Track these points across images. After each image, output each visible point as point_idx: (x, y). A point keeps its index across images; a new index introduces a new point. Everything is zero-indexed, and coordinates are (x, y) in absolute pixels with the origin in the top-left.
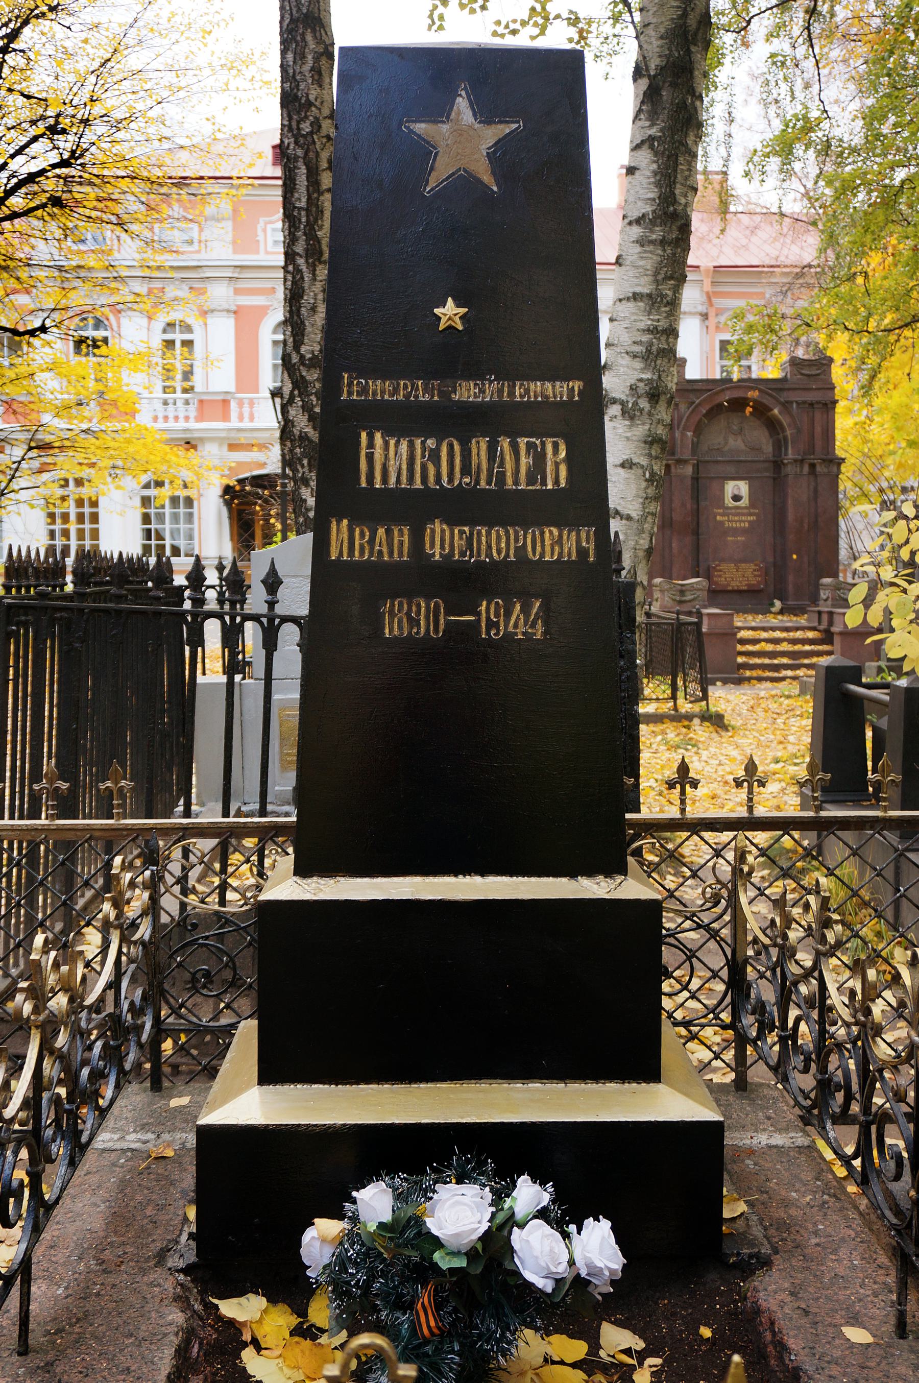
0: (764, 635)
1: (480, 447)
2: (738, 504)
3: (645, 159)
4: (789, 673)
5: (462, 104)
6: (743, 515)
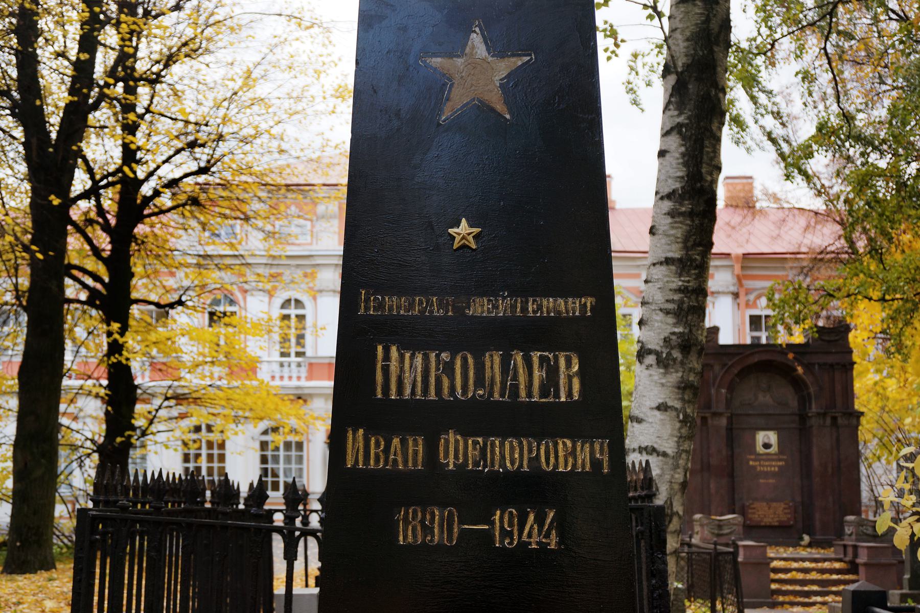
0: (795, 565)
1: (493, 361)
3: (674, 142)
4: (819, 599)
5: (476, 39)
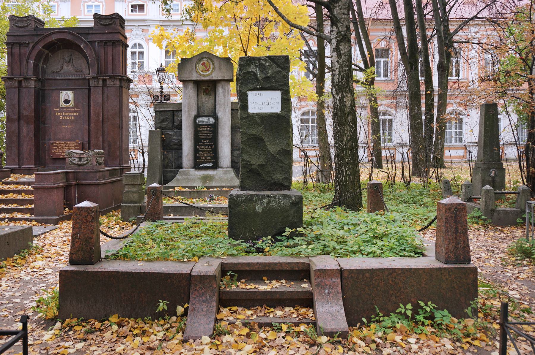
6: (71, 112)
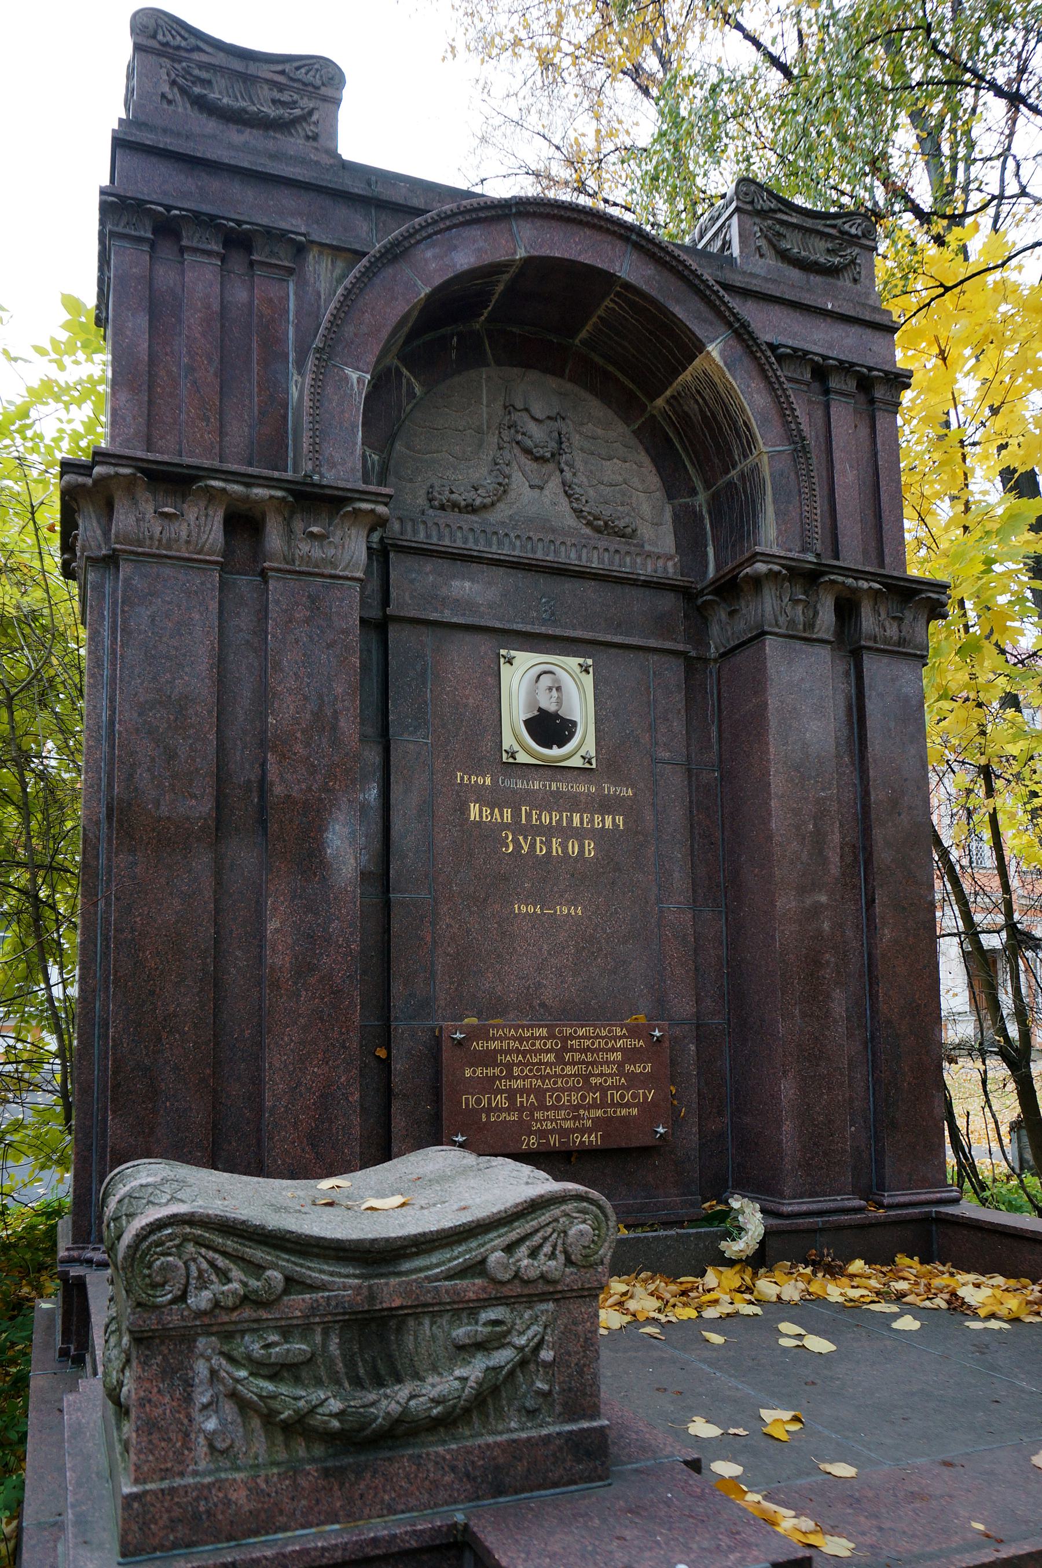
2: (555, 752)
6: (574, 803)
